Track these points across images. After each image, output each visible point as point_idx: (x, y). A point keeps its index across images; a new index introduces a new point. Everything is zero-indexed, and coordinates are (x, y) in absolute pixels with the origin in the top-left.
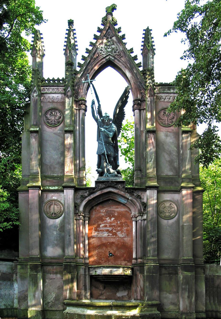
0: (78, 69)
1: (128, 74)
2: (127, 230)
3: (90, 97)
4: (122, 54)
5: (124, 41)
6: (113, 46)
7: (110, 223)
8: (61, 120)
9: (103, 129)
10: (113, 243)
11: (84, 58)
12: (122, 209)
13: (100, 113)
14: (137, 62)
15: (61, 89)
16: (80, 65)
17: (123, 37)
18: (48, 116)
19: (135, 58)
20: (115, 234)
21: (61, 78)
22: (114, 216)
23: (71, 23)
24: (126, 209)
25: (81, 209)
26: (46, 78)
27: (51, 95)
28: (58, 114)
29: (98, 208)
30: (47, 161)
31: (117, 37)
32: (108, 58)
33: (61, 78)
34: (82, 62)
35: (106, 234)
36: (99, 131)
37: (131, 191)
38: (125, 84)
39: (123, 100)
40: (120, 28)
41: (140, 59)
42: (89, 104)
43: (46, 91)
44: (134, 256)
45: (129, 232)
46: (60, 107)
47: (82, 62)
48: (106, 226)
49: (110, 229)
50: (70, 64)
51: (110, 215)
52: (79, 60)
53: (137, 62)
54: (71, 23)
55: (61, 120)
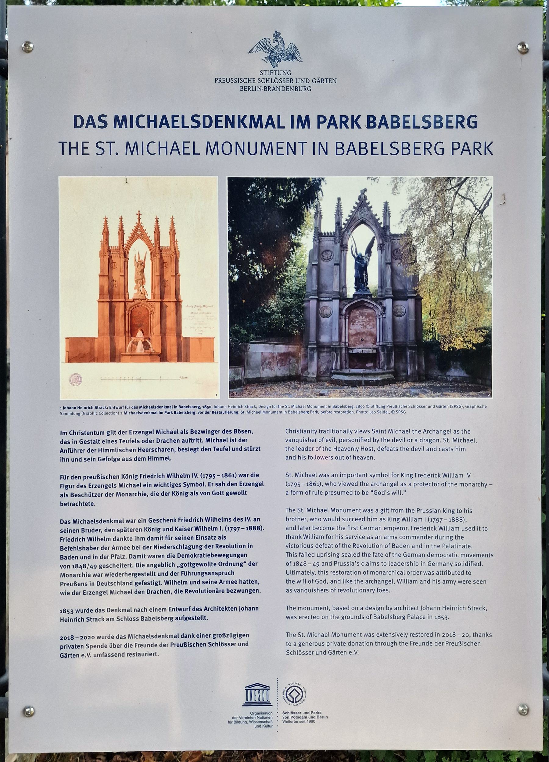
0: (343, 226)
1: (375, 229)
2: (373, 324)
3: (350, 243)
4: (370, 217)
5: (371, 209)
6: (365, 213)
7: (362, 320)
8: (332, 257)
9: (358, 262)
10: (364, 332)
11: (347, 220)
12: (370, 311)
13: (356, 252)
14: (379, 222)
15: (332, 239)
16: (344, 224)
17: (371, 207)
18: (324, 255)
19: (379, 219)
20: (366, 327)
21: (332, 232)
22: (364, 315)
23: (339, 199)
24: (373, 311)
25: (344, 312)
26: (323, 232)
27: (326, 242)
28: (330, 254)
29: (354, 311)
30: (323, 282)
31: (368, 207)
32: (361, 219)
33: (332, 232)
34: (346, 222)
35: (359, 327)
36: (356, 264)
37: (376, 300)
38: (373, 235)
39: (371, 245)
40: (369, 202)
41: (381, 220)
42: (349, 247)
43: (323, 240)
44: (378, 341)
45: (374, 326)
46: (331, 250)
47: (346, 222)
48: (359, 322)
49: (362, 323)
50: (338, 224)
51: (362, 314)
52: (344, 221)
53: (379, 222)
54: (339, 199)
55: (332, 257)
